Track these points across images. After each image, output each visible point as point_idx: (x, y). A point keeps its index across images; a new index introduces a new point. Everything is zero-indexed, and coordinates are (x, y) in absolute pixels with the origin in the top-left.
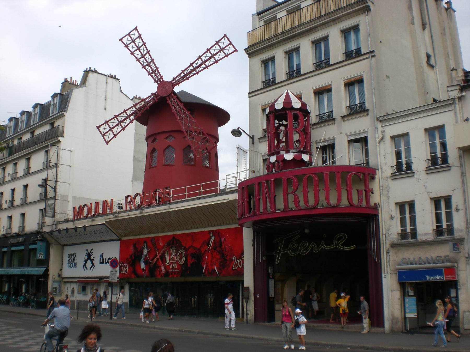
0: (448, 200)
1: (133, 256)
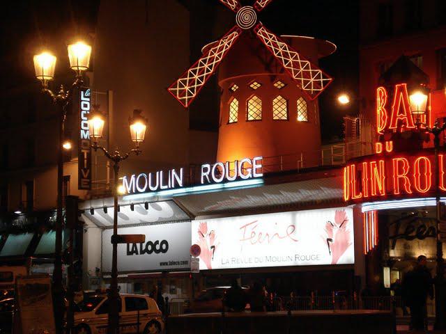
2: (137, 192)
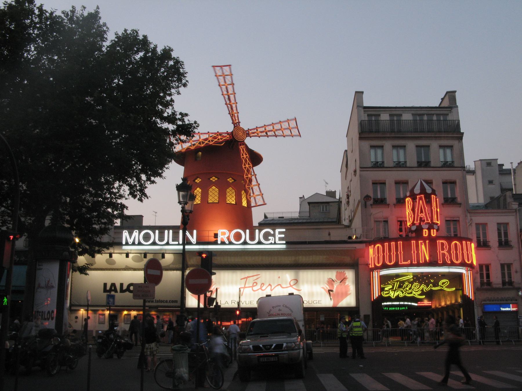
0: (509, 266)
2: (140, 244)
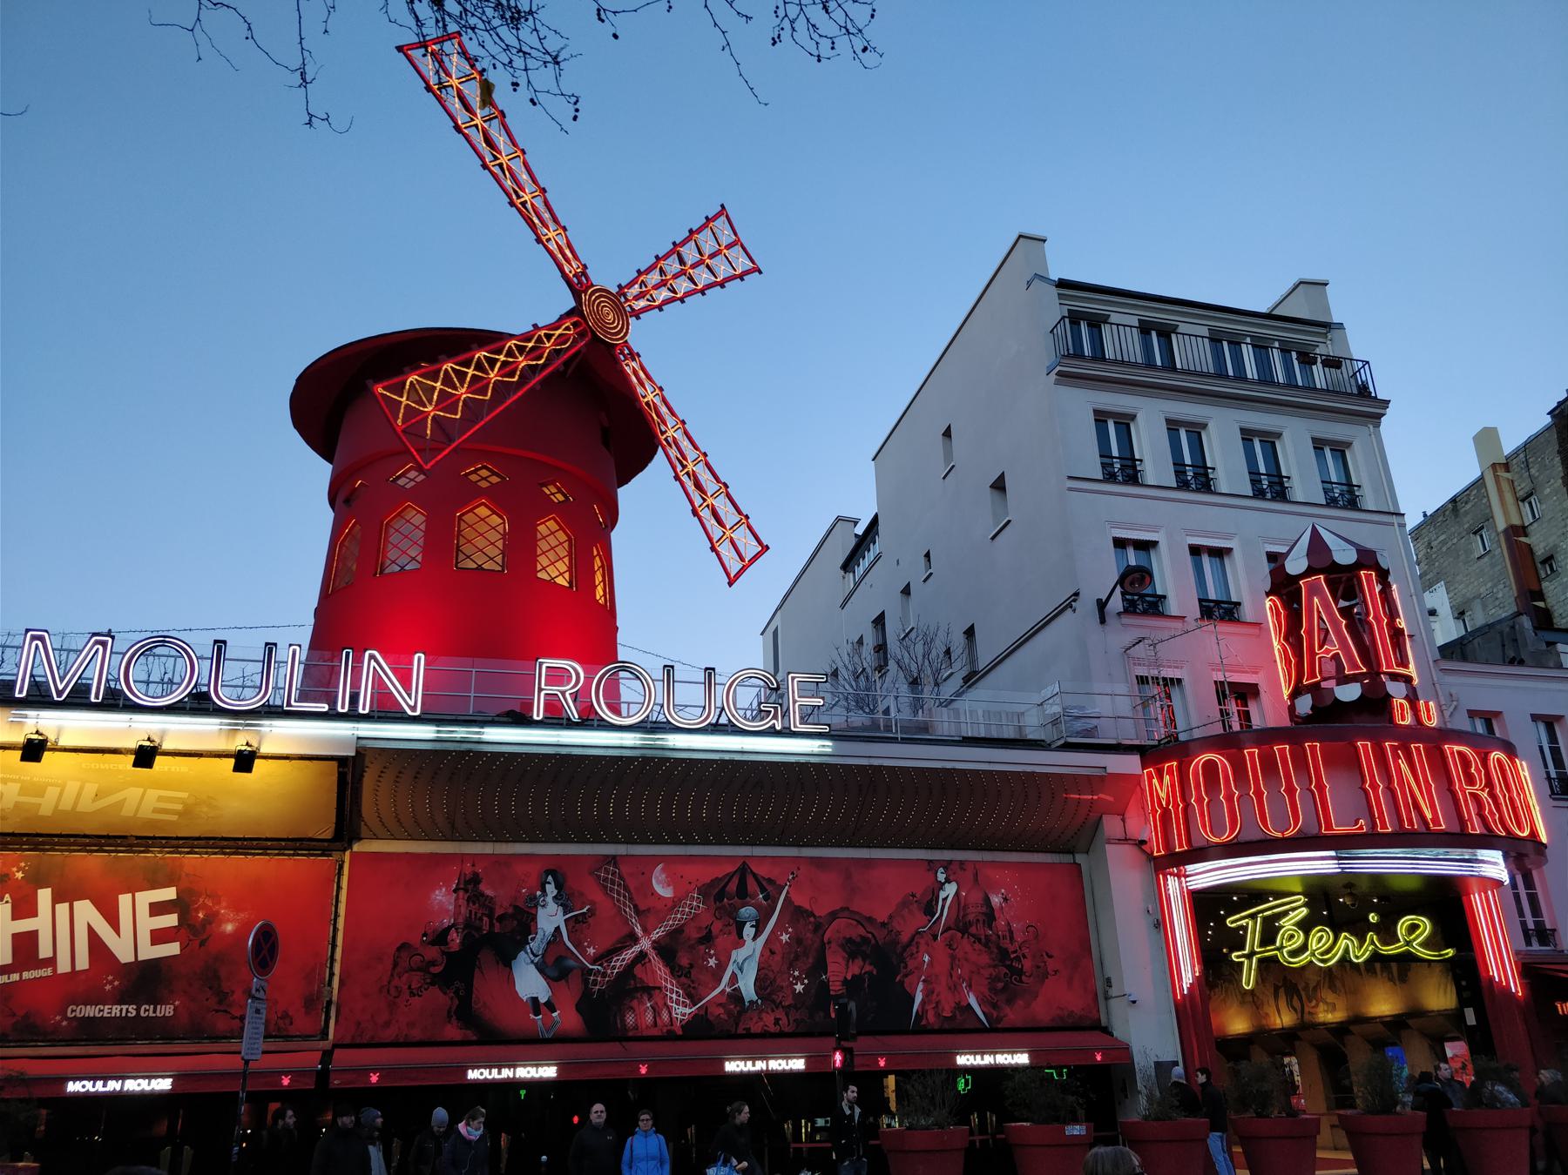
1: (455, 939)
